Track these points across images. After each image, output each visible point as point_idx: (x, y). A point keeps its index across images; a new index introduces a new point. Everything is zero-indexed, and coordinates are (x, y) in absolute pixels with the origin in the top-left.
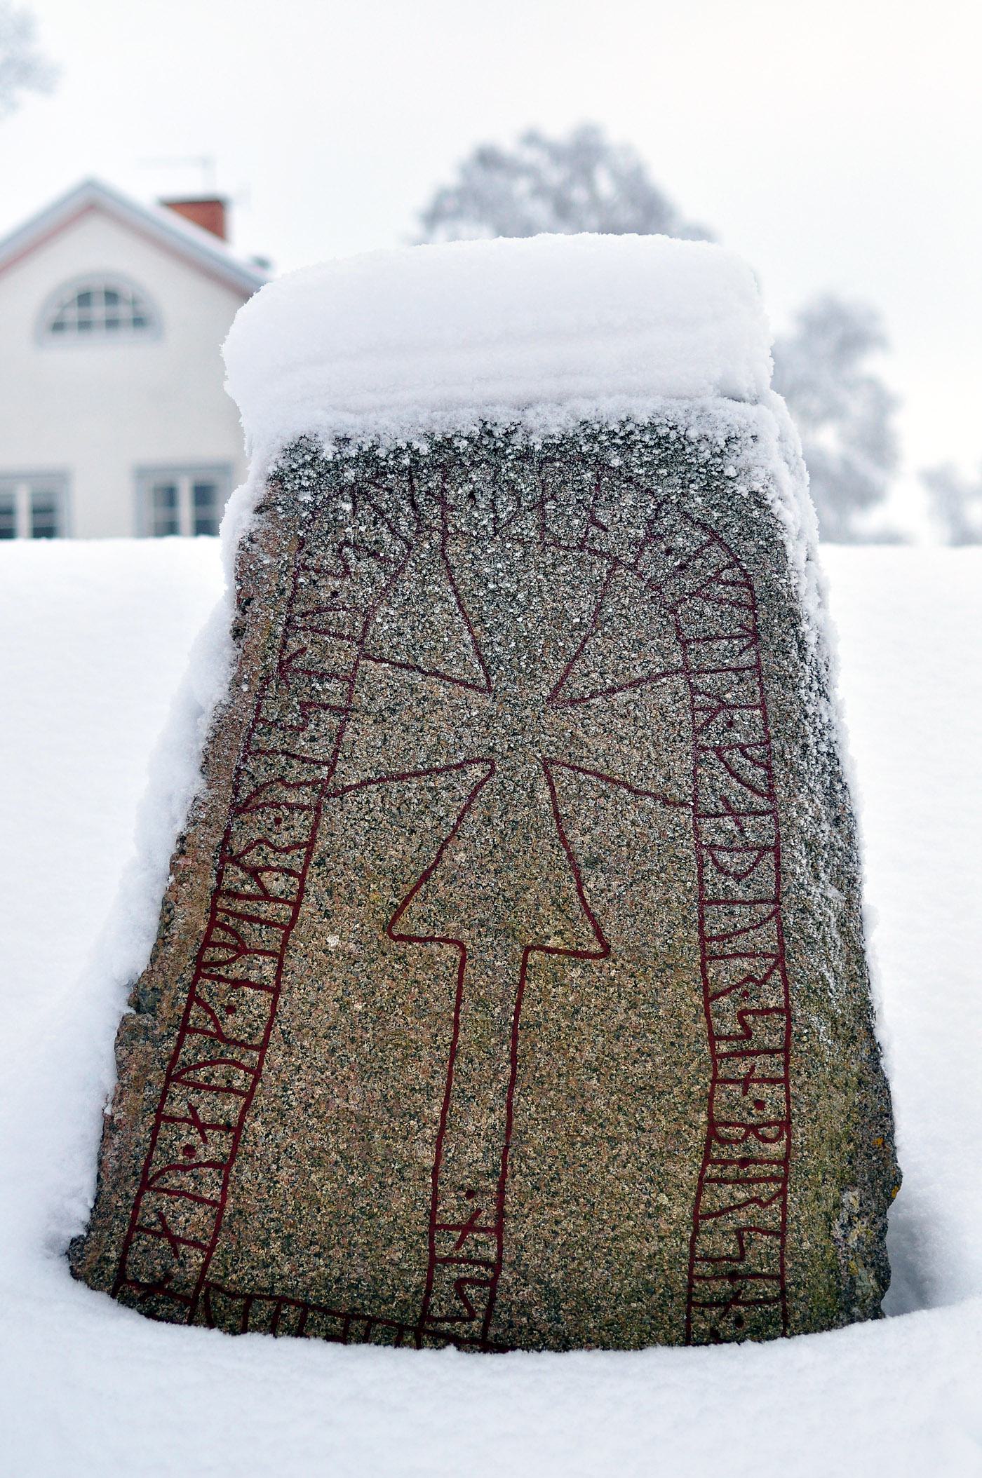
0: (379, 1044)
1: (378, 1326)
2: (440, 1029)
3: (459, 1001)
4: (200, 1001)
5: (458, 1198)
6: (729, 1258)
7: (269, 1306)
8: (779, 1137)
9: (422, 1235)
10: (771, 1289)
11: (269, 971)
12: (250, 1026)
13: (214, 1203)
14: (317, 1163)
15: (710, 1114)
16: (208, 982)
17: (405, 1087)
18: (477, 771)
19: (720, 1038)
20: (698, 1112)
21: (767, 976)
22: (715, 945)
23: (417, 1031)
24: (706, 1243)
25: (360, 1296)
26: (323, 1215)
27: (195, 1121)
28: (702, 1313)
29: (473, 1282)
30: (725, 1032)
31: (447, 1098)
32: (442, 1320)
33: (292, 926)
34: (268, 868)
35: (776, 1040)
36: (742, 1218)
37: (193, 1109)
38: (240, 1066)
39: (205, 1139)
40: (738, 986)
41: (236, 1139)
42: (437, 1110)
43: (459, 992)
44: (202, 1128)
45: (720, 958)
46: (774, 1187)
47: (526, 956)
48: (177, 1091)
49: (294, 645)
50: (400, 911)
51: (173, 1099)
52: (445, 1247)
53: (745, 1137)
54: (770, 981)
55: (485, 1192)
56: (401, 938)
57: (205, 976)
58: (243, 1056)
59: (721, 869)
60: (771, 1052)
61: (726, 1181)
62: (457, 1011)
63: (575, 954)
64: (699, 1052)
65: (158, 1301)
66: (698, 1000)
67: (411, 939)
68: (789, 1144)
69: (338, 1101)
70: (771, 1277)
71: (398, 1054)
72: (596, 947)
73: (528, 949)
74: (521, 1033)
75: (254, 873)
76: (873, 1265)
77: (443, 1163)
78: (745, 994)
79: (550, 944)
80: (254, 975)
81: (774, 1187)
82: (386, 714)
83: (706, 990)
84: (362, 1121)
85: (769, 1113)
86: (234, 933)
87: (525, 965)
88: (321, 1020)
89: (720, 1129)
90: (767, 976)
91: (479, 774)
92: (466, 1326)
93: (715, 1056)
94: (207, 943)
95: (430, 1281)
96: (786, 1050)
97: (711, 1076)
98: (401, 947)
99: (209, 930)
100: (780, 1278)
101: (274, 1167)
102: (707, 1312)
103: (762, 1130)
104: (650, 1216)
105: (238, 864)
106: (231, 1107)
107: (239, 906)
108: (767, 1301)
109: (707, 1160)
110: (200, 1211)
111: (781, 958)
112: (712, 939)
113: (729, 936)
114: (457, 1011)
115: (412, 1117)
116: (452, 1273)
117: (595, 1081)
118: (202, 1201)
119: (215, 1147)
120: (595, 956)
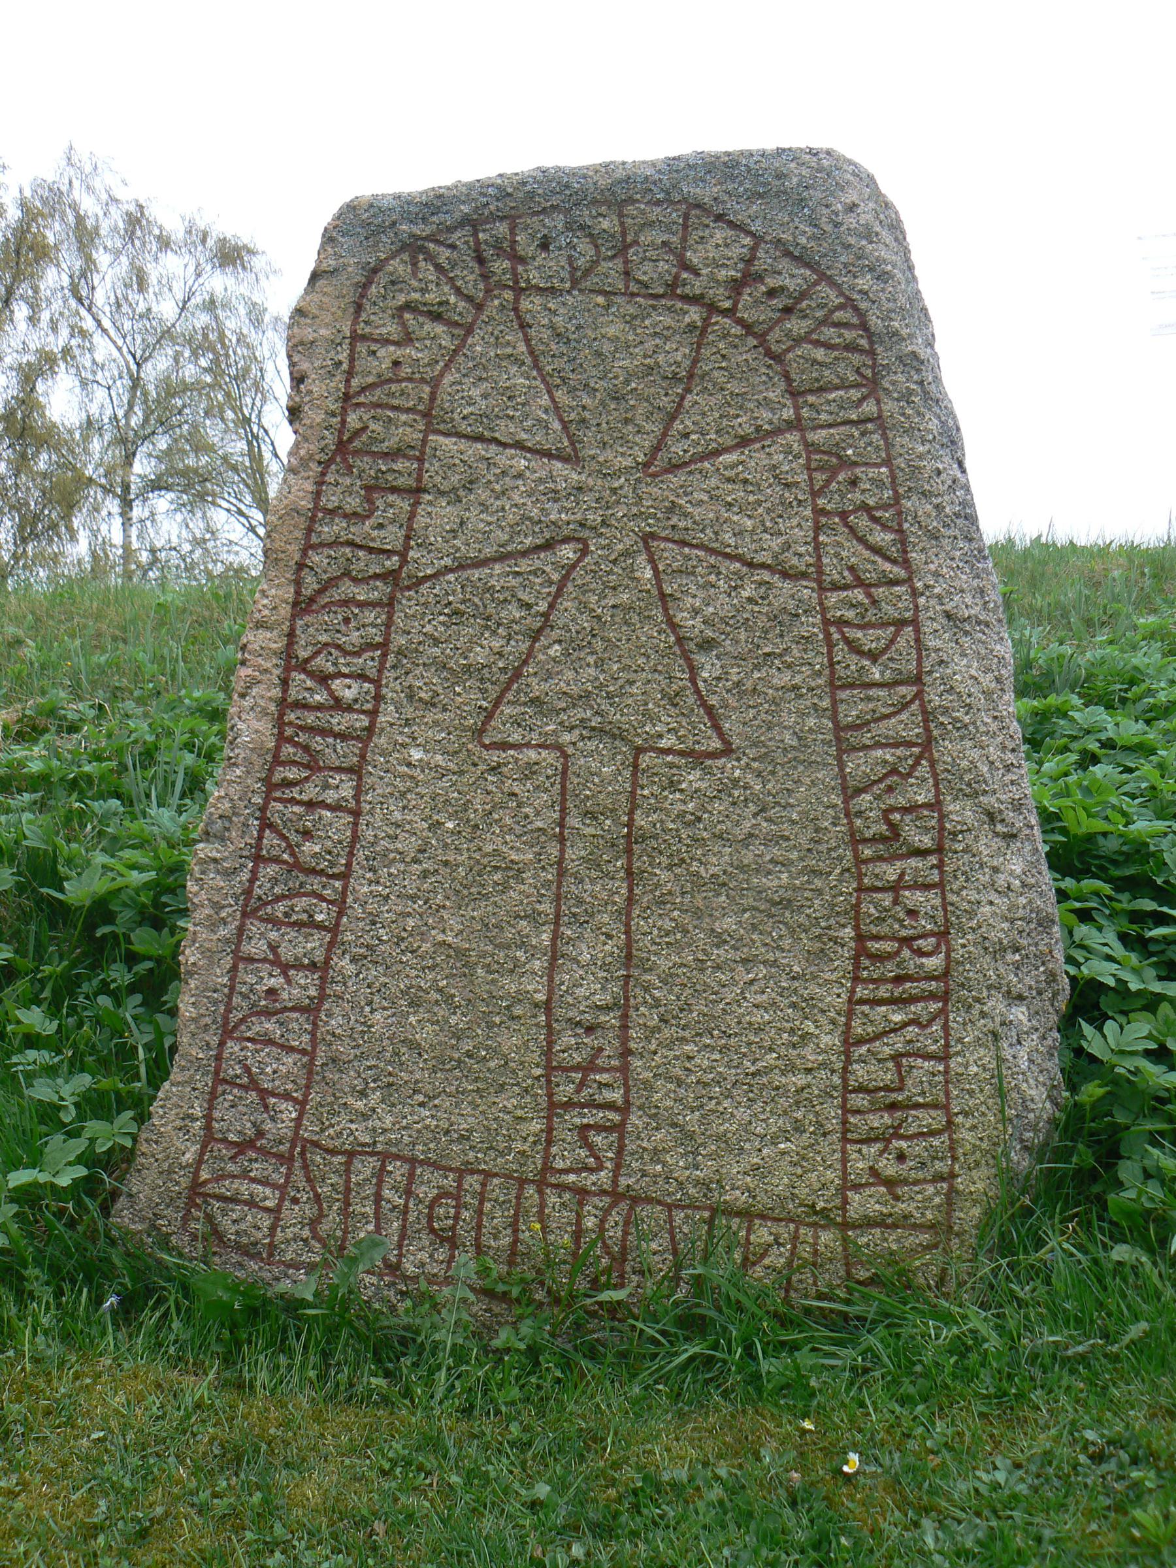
3: (563, 811)
4: (271, 826)
6: (887, 1089)
9: (537, 1078)
11: (347, 791)
12: (330, 853)
13: (303, 1052)
15: (856, 928)
18: (567, 552)
22: (853, 738)
25: (472, 1148)
27: (276, 962)
28: (860, 1151)
29: (599, 1128)
30: (868, 834)
33: (370, 738)
34: (340, 675)
35: (927, 841)
36: (897, 1043)
37: (273, 948)
38: (322, 898)
39: (289, 981)
40: (880, 780)
43: (564, 801)
44: (285, 968)
45: (859, 750)
47: (636, 758)
49: (353, 419)
50: (490, 716)
52: (565, 1091)
53: (898, 953)
56: (495, 746)
57: (276, 800)
58: (324, 887)
60: (922, 853)
64: (840, 858)
67: (504, 746)
68: (948, 956)
72: (716, 744)
73: (639, 751)
75: (324, 679)
77: (556, 998)
79: (663, 743)
80: (331, 796)
81: (934, 1006)
82: (461, 493)
83: (844, 788)
86: (306, 748)
87: (635, 766)
89: (869, 944)
90: (913, 767)
91: (571, 555)
92: (593, 1178)
93: (859, 861)
94: (277, 761)
96: (939, 850)
98: (495, 757)
99: (278, 748)
101: (367, 1009)
102: (864, 1149)
105: (304, 671)
106: (313, 945)
107: (310, 718)
110: (289, 1060)
114: (562, 825)
115: (519, 947)
118: (291, 1050)
119: (304, 986)
120: (713, 755)
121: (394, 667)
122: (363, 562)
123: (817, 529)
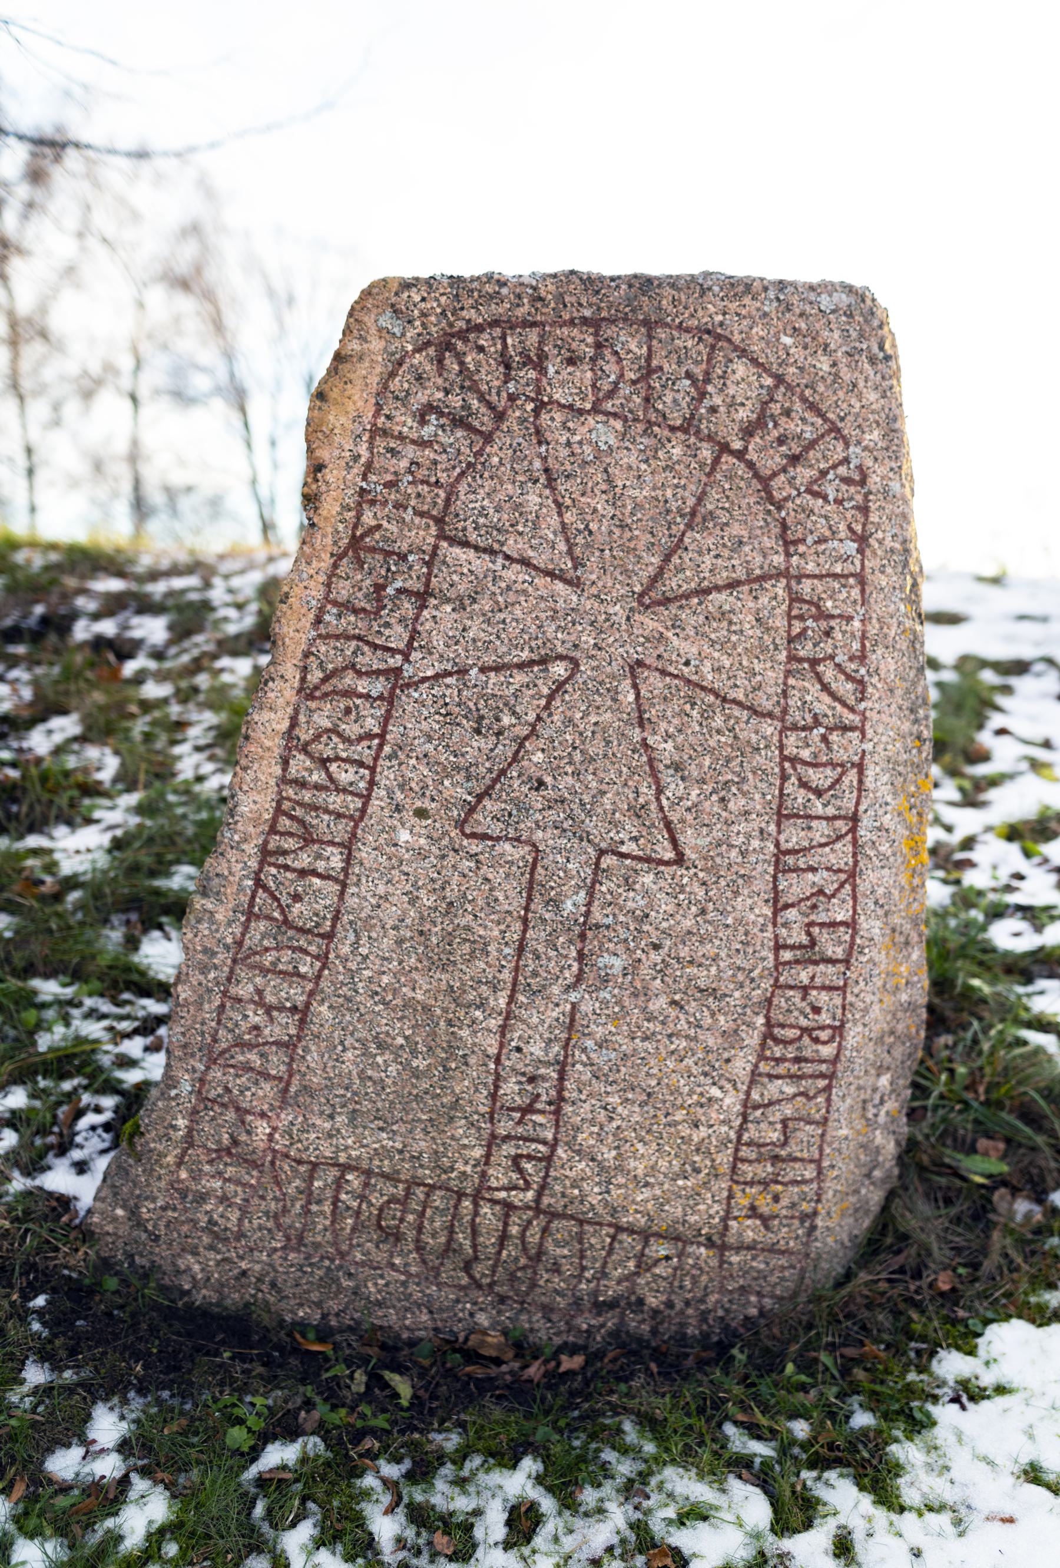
0: (448, 937)
1: (438, 1192)
2: (508, 926)
3: (530, 899)
4: (266, 888)
5: (520, 1083)
6: (773, 1144)
7: (334, 1172)
8: (831, 1040)
9: (483, 1116)
10: (810, 1173)
11: (336, 862)
12: (317, 915)
13: (280, 1079)
14: (382, 1046)
15: (767, 1017)
16: (273, 871)
17: (472, 979)
18: (559, 670)
19: (786, 947)
20: (757, 1014)
21: (838, 890)
22: (790, 860)
23: (486, 927)
24: (751, 1133)
25: (421, 1166)
26: (388, 1094)
27: (260, 1003)
28: (743, 1191)
29: (529, 1157)
30: (790, 942)
31: (514, 991)
32: (498, 1189)
33: (361, 818)
34: (338, 758)
35: (839, 952)
36: (788, 1111)
37: (260, 992)
38: (306, 952)
39: (272, 1019)
40: (808, 898)
41: (302, 1021)
42: (502, 1002)
43: (530, 889)
44: (269, 1009)
45: (794, 871)
46: (822, 1083)
47: (598, 859)
48: (243, 974)
49: (368, 518)
50: (472, 810)
51: (238, 982)
52: (504, 1127)
53: (800, 1038)
54: (838, 895)
55: (544, 1078)
56: (473, 835)
57: (270, 864)
58: (310, 943)
59: (804, 784)
60: (833, 961)
61: (778, 1077)
62: (527, 909)
63: (648, 860)
64: (764, 959)
65: (226, 1164)
66: (768, 912)
67: (485, 837)
68: (840, 1048)
69: (404, 989)
70: (811, 1161)
71: (466, 948)
72: (670, 855)
73: (602, 853)
74: (590, 934)
75: (324, 763)
76: (894, 1133)
77: (504, 1051)
78: (814, 907)
79: (624, 849)
80: (321, 866)
81: (822, 1083)
82: (467, 602)
83: (776, 900)
84: (427, 1009)
85: (825, 1018)
86: (301, 822)
87: (597, 864)
88: (390, 913)
89: (776, 1031)
90: (838, 890)
91: (562, 672)
92: (521, 1196)
93: (778, 964)
94: (273, 830)
95: (488, 1155)
96: (847, 962)
97: (772, 982)
98: (475, 846)
99: (274, 820)
100: (818, 1162)
101: (340, 1048)
102: (748, 1190)
103: (815, 1034)
104: (702, 1106)
105: (307, 753)
106: (297, 994)
107: (307, 796)
108: (804, 1182)
109: (761, 1057)
110: (267, 1086)
111: (853, 874)
112: (788, 852)
113: (804, 850)
114: (527, 909)
115: (478, 1007)
116: (509, 1149)
117: (658, 981)
118: (267, 1077)
119: (284, 1026)
120: (667, 863)
121: (389, 758)
122: (368, 659)
123: (788, 673)
